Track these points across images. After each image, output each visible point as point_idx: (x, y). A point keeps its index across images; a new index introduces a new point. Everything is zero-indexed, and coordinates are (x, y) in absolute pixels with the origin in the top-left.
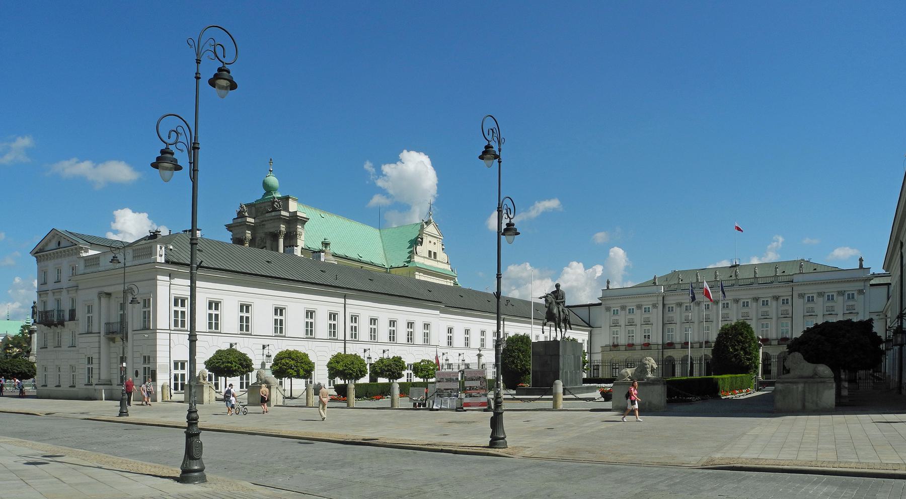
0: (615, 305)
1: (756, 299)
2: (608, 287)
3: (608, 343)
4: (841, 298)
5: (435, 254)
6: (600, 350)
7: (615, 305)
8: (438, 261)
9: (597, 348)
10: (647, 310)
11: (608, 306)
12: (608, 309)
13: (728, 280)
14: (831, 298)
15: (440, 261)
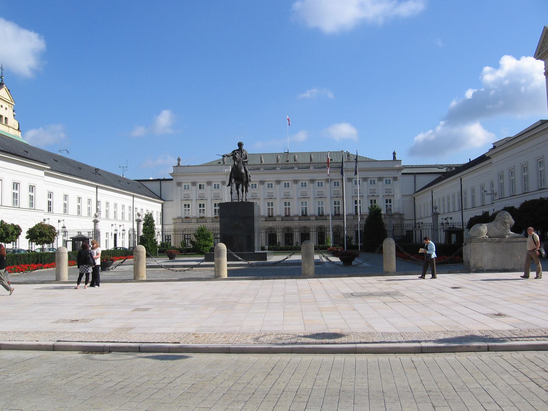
0: (186, 181)
1: (296, 182)
2: (179, 164)
3: (180, 216)
4: (380, 183)
5: (6, 118)
6: (172, 222)
7: (186, 181)
8: (9, 127)
9: (169, 220)
10: (217, 187)
11: (178, 181)
12: (179, 184)
13: (286, 164)
14: (373, 182)
15: (11, 127)
